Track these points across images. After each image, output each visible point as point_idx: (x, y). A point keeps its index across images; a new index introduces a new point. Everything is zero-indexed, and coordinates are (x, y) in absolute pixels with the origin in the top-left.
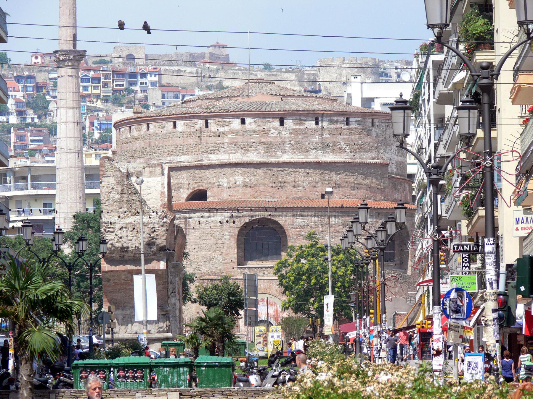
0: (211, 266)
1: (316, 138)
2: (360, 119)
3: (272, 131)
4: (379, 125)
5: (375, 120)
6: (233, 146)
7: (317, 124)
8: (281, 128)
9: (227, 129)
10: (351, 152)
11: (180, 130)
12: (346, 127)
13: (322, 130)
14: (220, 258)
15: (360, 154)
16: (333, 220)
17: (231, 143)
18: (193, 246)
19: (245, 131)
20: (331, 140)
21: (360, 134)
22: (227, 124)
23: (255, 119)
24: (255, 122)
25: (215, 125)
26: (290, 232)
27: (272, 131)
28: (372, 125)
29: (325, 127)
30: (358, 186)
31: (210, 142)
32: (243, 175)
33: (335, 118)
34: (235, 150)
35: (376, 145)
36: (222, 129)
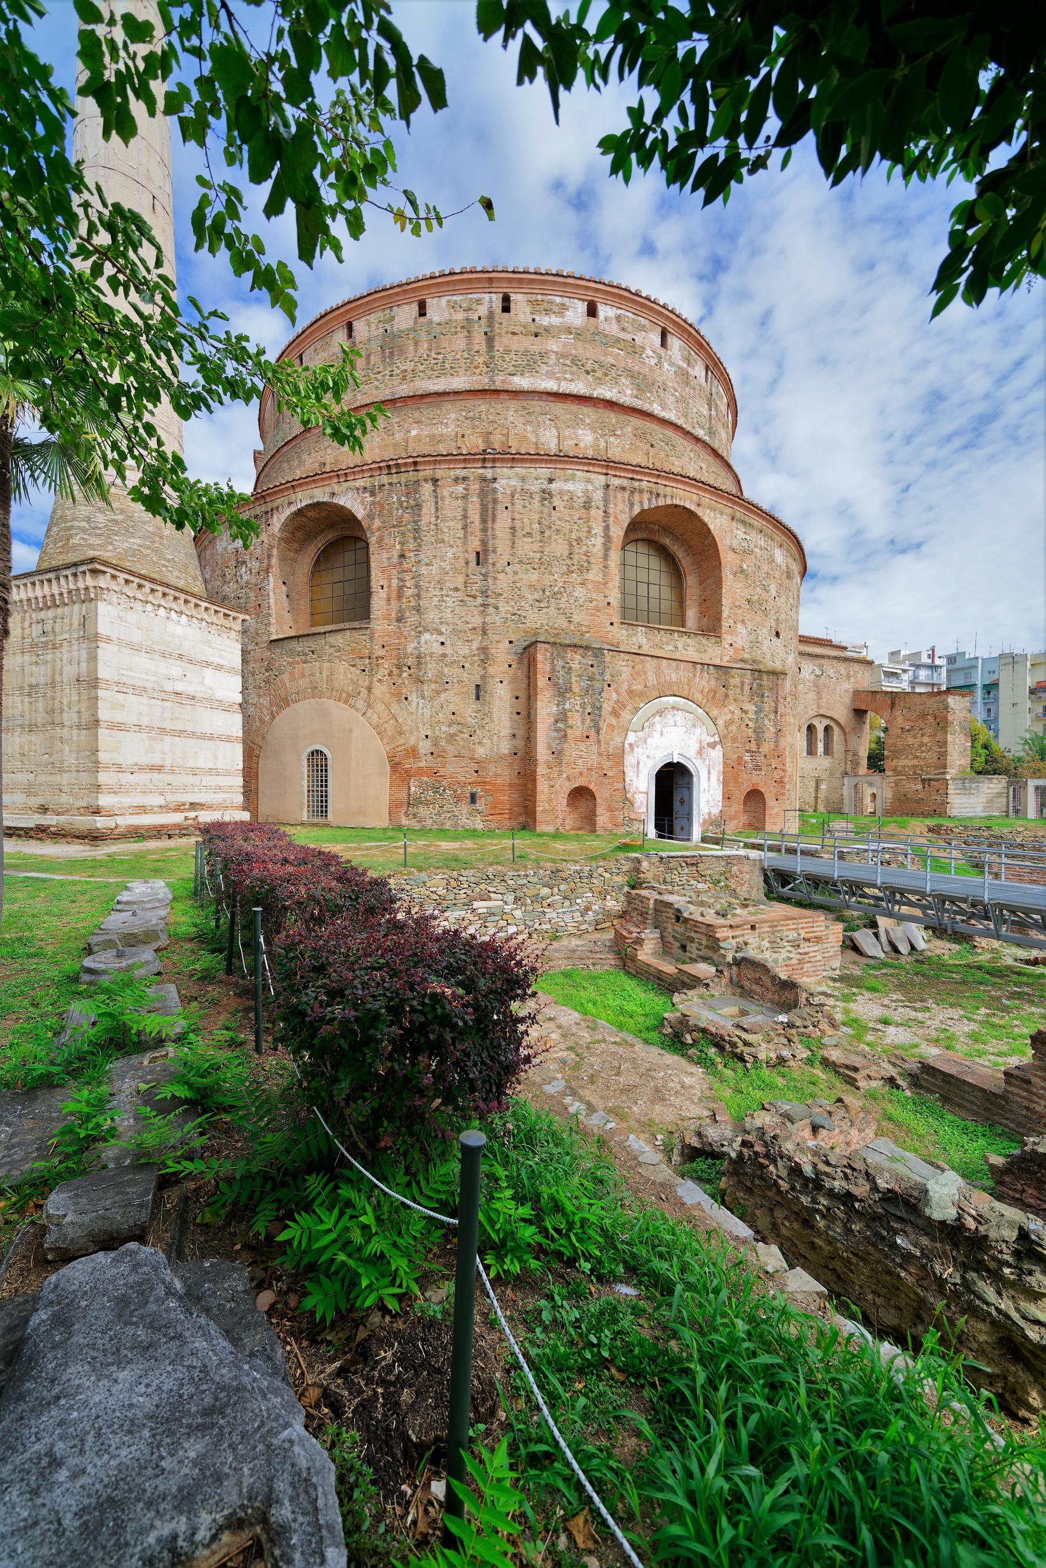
0: (552, 612)
3: (649, 352)
6: (568, 362)
8: (662, 351)
9: (554, 320)
11: (436, 319)
14: (579, 592)
17: (564, 356)
18: (506, 557)
19: (597, 333)
22: (556, 309)
23: (619, 312)
24: (618, 318)
25: (528, 310)
26: (728, 559)
27: (649, 352)
31: (514, 348)
32: (593, 430)
34: (572, 373)
36: (545, 320)
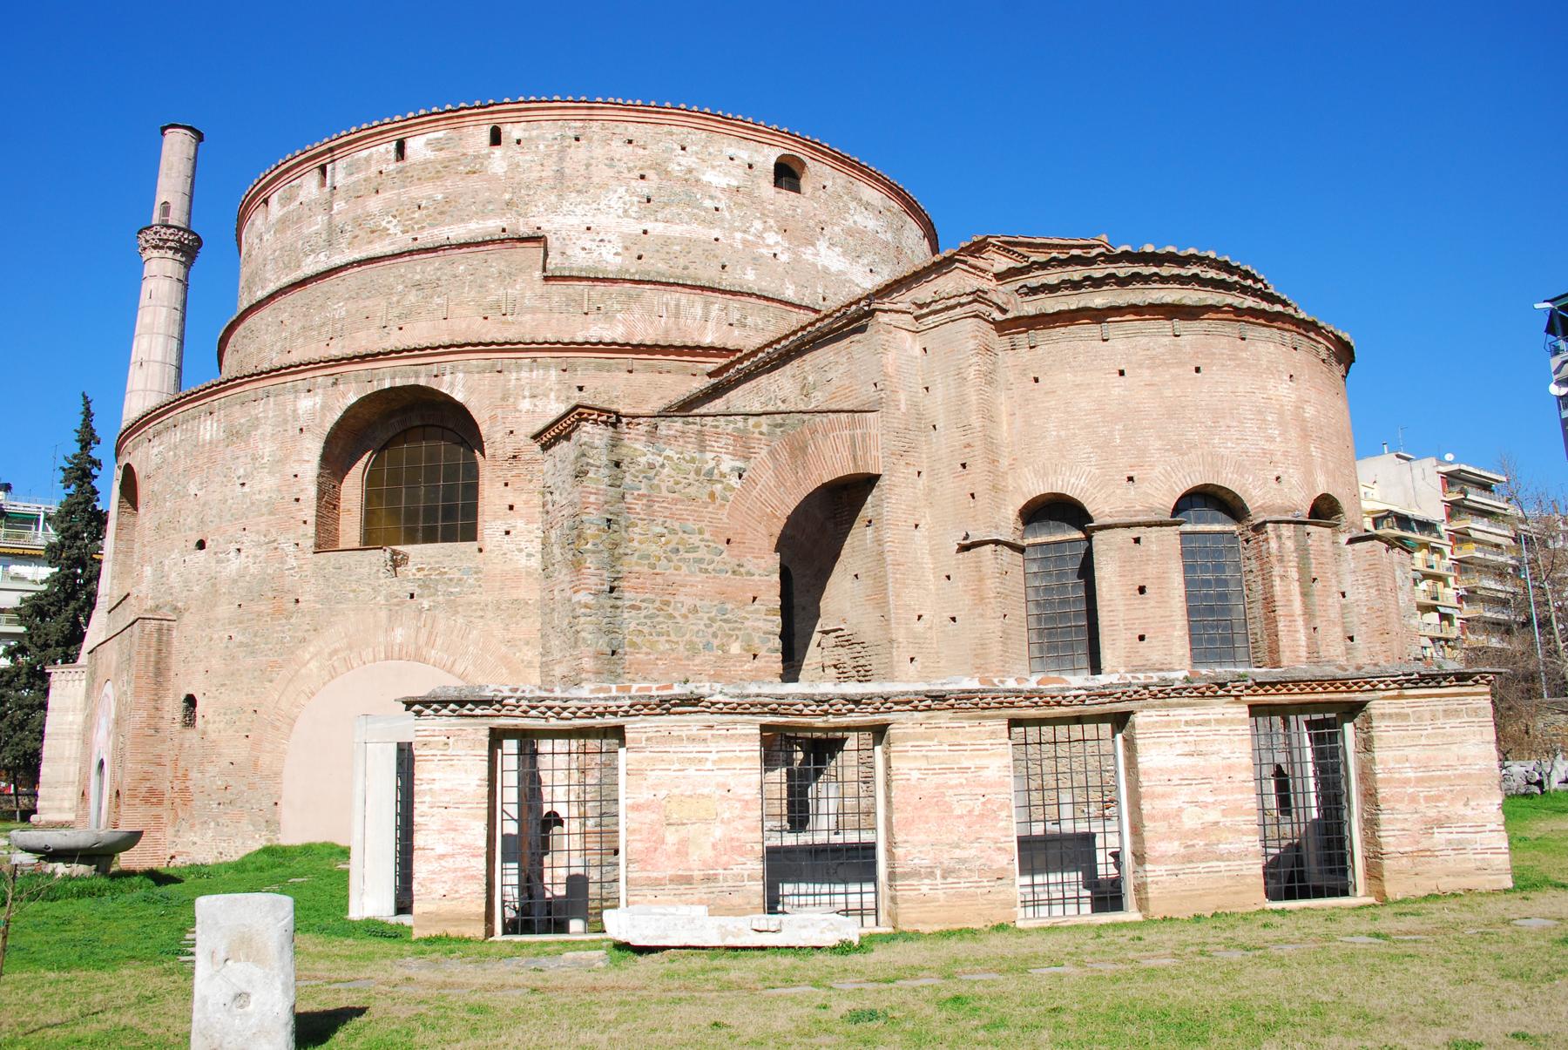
1: (320, 220)
2: (440, 134)
4: (530, 139)
5: (505, 129)
7: (323, 184)
10: (404, 232)
12: (393, 166)
13: (332, 195)
15: (436, 232)
16: (209, 430)
20: (352, 215)
21: (438, 176)
28: (496, 138)
29: (338, 185)
30: (401, 324)
33: (365, 153)
35: (507, 196)
